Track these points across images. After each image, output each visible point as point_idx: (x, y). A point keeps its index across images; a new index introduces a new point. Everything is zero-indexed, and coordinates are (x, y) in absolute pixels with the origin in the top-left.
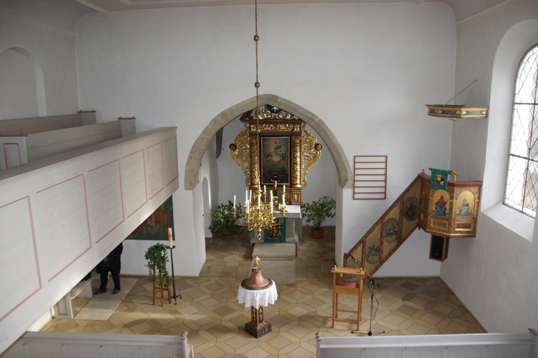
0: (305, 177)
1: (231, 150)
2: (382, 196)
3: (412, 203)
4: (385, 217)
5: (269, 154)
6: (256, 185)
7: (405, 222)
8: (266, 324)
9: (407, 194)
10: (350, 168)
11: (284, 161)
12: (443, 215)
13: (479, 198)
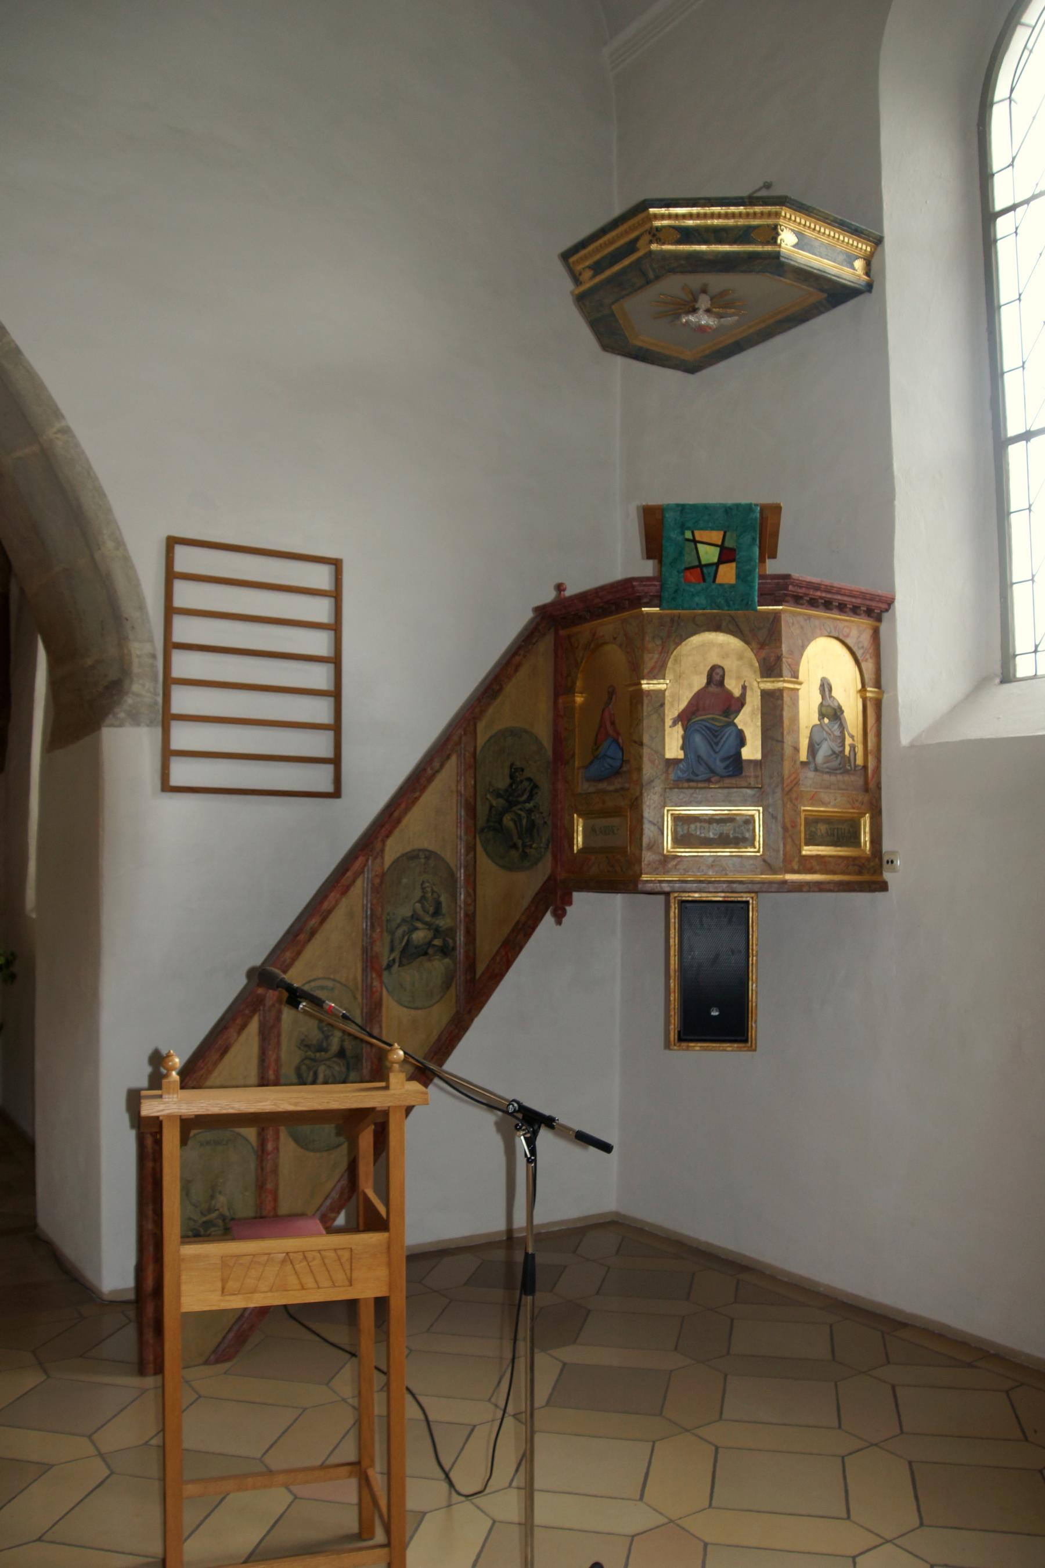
2: (320, 778)
3: (518, 764)
4: (384, 842)
10: (142, 607)
12: (729, 776)
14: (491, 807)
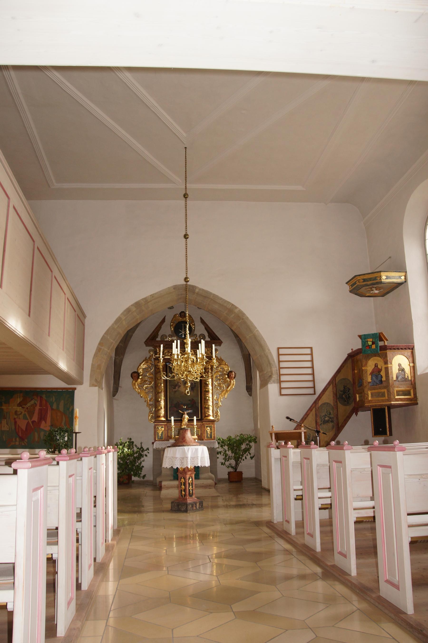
0: (218, 410)
1: (133, 380)
3: (345, 385)
4: (318, 401)
5: (177, 384)
6: (161, 417)
7: (342, 408)
8: (195, 499)
9: (339, 375)
10: (274, 361)
11: (193, 392)
13: (414, 362)
14: (340, 394)
